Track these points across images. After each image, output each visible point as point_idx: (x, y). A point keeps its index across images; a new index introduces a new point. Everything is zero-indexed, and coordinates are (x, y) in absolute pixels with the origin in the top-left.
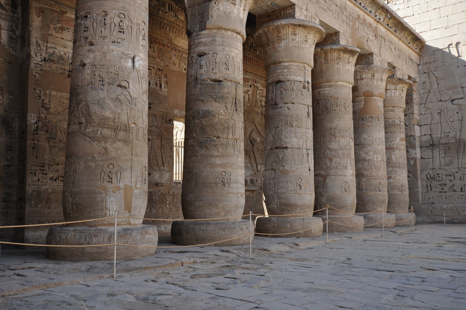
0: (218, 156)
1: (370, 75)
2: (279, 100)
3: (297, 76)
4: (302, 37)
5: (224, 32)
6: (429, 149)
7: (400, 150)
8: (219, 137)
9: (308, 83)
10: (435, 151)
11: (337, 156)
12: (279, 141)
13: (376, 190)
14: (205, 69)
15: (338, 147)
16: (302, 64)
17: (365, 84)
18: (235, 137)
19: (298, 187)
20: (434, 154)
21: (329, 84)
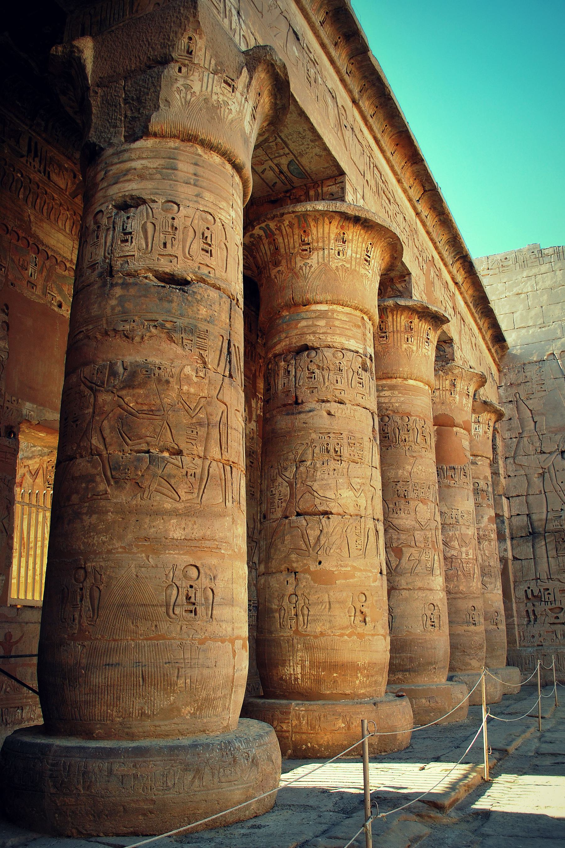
0: (175, 513)
1: (447, 382)
2: (304, 393)
3: (349, 338)
4: (359, 250)
5: (200, 150)
6: (527, 541)
7: (490, 541)
8: (179, 453)
9: (371, 358)
10: (539, 546)
11: (413, 544)
12: (307, 496)
13: (468, 623)
14: (138, 241)
15: (414, 523)
16: (358, 313)
17: (438, 400)
18: (226, 456)
19: (359, 618)
20: (538, 552)
21: (389, 382)
